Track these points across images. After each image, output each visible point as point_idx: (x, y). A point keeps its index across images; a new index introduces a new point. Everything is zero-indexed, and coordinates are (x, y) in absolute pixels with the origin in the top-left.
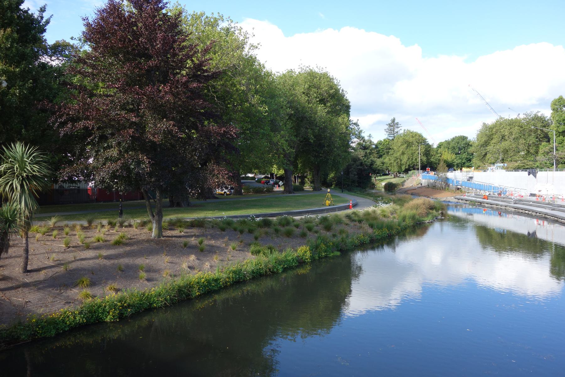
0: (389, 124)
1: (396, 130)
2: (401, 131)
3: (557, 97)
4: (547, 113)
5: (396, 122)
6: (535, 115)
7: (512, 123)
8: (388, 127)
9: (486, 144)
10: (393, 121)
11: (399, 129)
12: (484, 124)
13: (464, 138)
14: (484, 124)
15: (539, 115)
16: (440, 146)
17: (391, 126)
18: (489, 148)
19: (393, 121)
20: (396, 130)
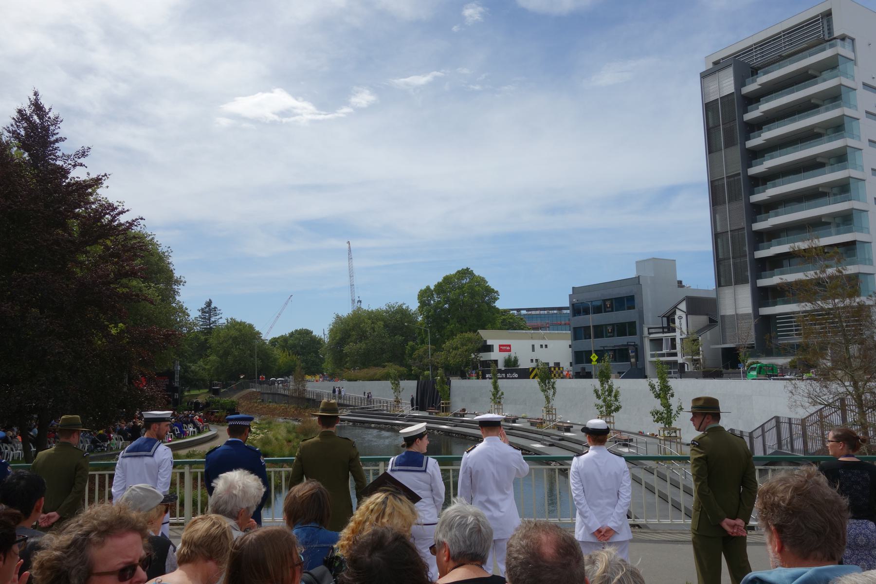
0: (202, 309)
1: (213, 319)
2: (222, 319)
3: (424, 288)
4: (413, 305)
5: (213, 306)
6: (401, 306)
7: (375, 317)
8: (200, 313)
10: (209, 304)
12: (338, 316)
13: (306, 333)
14: (338, 316)
15: (404, 307)
16: (274, 341)
17: (205, 312)
18: (346, 349)
19: (209, 304)
20: (213, 319)
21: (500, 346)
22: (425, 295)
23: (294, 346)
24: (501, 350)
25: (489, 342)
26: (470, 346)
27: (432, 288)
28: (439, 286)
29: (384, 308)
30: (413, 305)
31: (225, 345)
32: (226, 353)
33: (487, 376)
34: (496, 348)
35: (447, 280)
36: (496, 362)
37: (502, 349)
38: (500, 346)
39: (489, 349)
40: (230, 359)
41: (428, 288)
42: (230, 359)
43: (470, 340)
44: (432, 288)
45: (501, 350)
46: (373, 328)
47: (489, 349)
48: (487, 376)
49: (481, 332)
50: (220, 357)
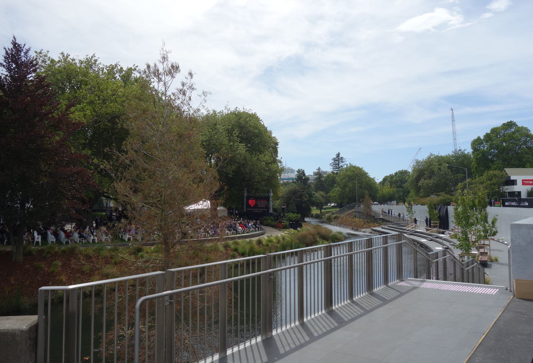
0: (334, 159)
3: (476, 138)
5: (340, 156)
9: (418, 179)
10: (338, 155)
11: (344, 163)
17: (336, 161)
18: (420, 184)
19: (338, 155)
20: (341, 164)
21: (523, 180)
22: (476, 143)
23: (396, 182)
24: (524, 184)
25: (513, 178)
26: (494, 181)
27: (482, 138)
28: (487, 136)
29: (451, 153)
30: (469, 150)
31: (344, 181)
32: (345, 186)
33: (506, 204)
34: (519, 182)
35: (494, 130)
36: (519, 193)
37: (524, 183)
38: (523, 180)
39: (514, 183)
40: (347, 189)
41: (479, 138)
42: (347, 189)
43: (495, 176)
44: (482, 138)
45: (524, 184)
46: (440, 169)
47: (514, 183)
48: (506, 204)
49: (508, 171)
50: (342, 188)
